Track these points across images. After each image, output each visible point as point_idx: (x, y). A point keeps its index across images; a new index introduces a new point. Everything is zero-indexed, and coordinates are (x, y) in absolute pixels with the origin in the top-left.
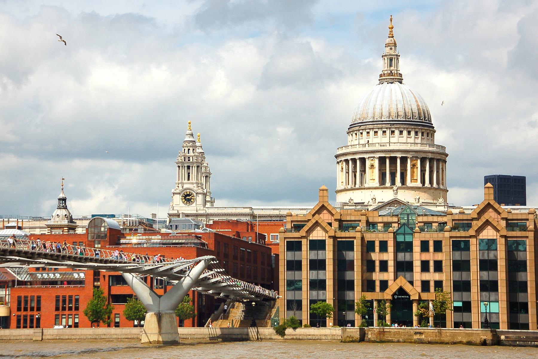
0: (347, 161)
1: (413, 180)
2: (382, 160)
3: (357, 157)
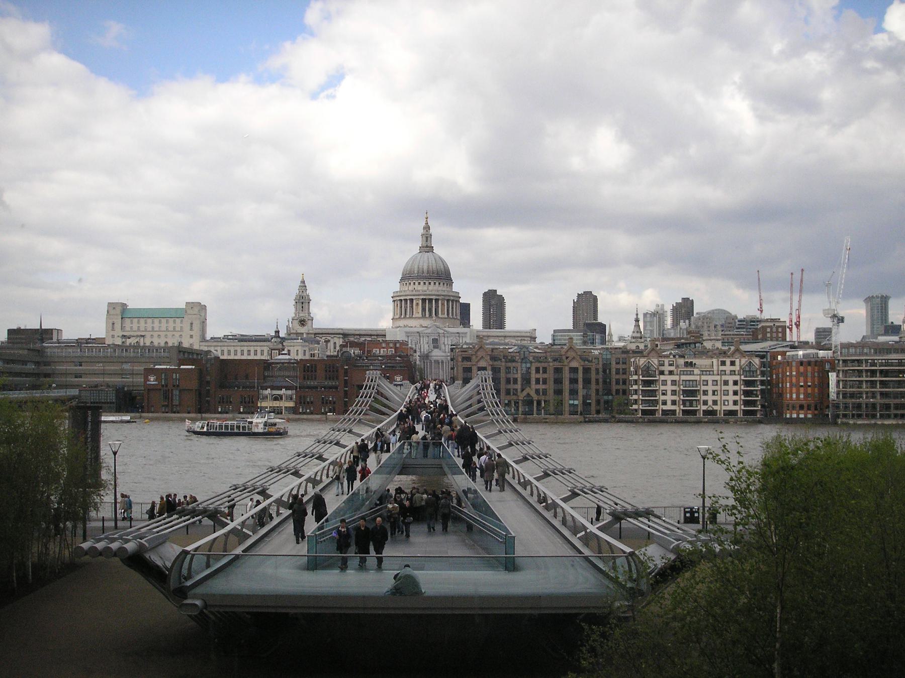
0: (401, 300)
1: (443, 313)
2: (424, 300)
3: (408, 298)
